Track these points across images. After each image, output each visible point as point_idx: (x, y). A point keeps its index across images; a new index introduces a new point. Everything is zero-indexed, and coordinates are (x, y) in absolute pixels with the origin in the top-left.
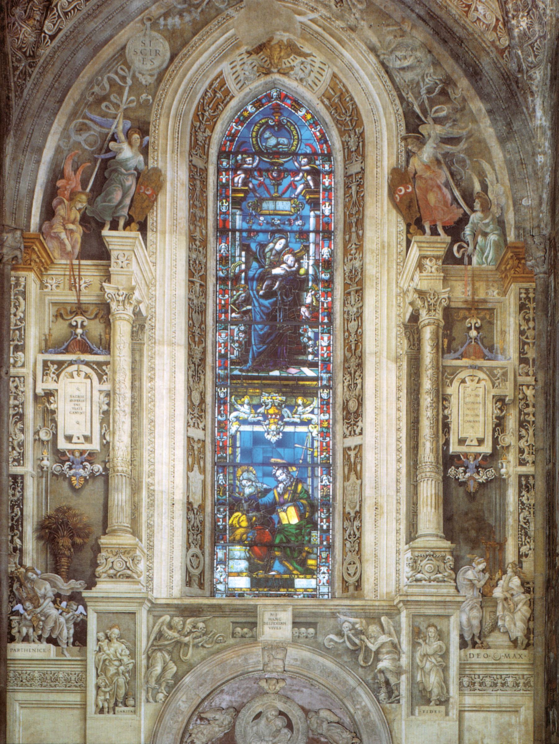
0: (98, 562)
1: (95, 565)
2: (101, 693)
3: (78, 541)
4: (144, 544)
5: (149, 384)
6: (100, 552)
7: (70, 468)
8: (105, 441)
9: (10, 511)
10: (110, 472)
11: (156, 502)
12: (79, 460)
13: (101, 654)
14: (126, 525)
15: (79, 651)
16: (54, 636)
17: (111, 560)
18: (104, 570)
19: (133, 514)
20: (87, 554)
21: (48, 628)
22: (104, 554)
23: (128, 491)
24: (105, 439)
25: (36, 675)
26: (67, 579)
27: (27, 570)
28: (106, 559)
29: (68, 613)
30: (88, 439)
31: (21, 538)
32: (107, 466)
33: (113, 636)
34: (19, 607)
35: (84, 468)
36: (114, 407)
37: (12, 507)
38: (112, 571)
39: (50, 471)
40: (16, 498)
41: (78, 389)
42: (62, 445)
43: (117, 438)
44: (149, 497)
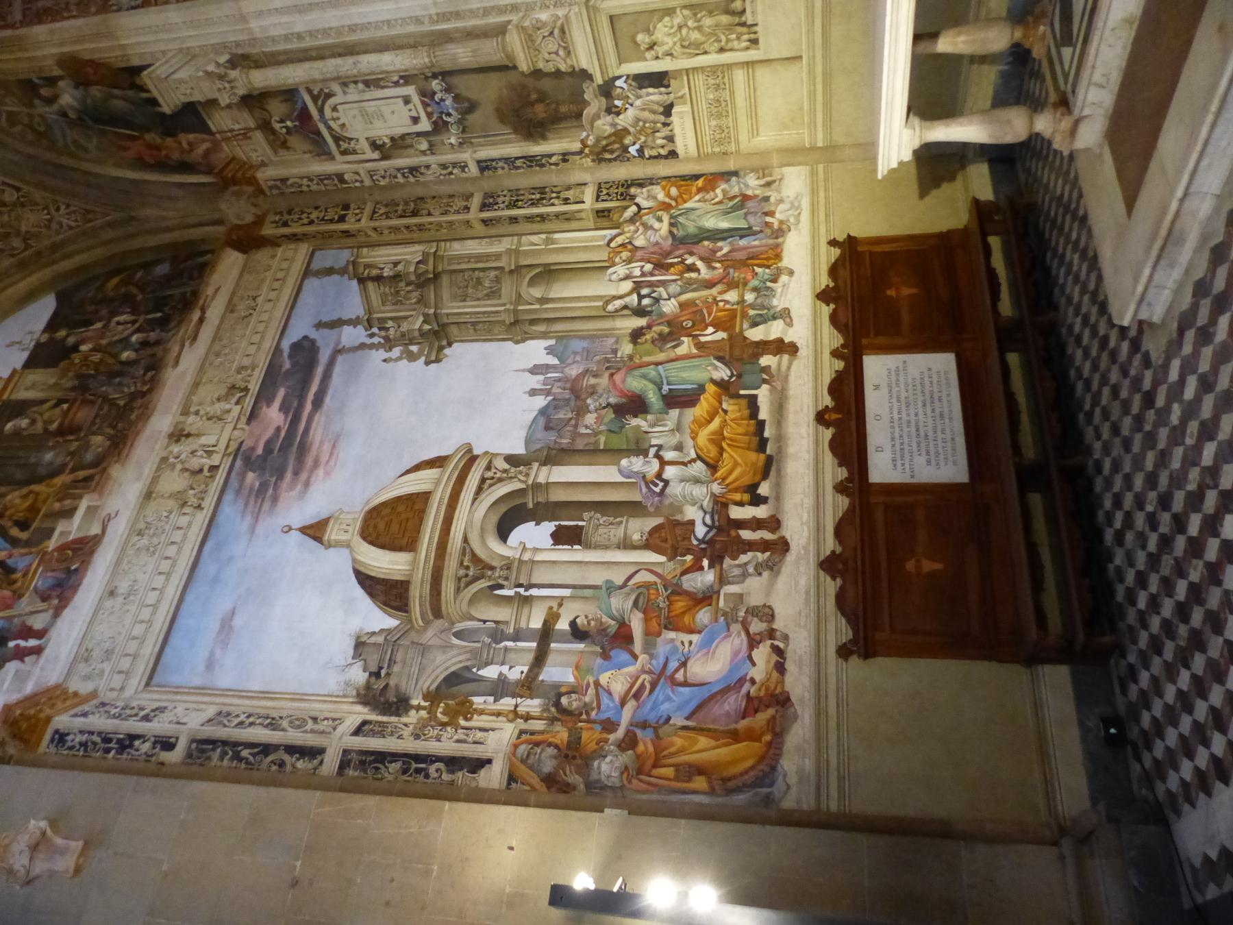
0: (553, 70)
1: (558, 74)
2: (730, 45)
3: (534, 96)
4: (514, 18)
5: (307, 39)
6: (540, 70)
7: (449, 115)
8: (401, 81)
9: (522, 170)
10: (436, 70)
11: (452, 9)
12: (435, 107)
13: (675, 53)
14: (495, 44)
15: (676, 79)
16: (661, 109)
17: (547, 56)
18: (562, 62)
19: (478, 36)
20: (547, 85)
21: (652, 117)
22: (541, 65)
23: (450, 46)
24: (398, 82)
25: (714, 123)
26: (585, 103)
27: (585, 146)
28: (547, 61)
29: (628, 97)
30: (407, 100)
31: (550, 156)
32: (430, 75)
33: (647, 40)
34: (633, 150)
35: (442, 100)
36: (355, 76)
37: (517, 168)
38: (561, 53)
39: (461, 135)
40: (506, 166)
41: (354, 117)
42: (425, 125)
43: (391, 68)
44: (449, 20)
